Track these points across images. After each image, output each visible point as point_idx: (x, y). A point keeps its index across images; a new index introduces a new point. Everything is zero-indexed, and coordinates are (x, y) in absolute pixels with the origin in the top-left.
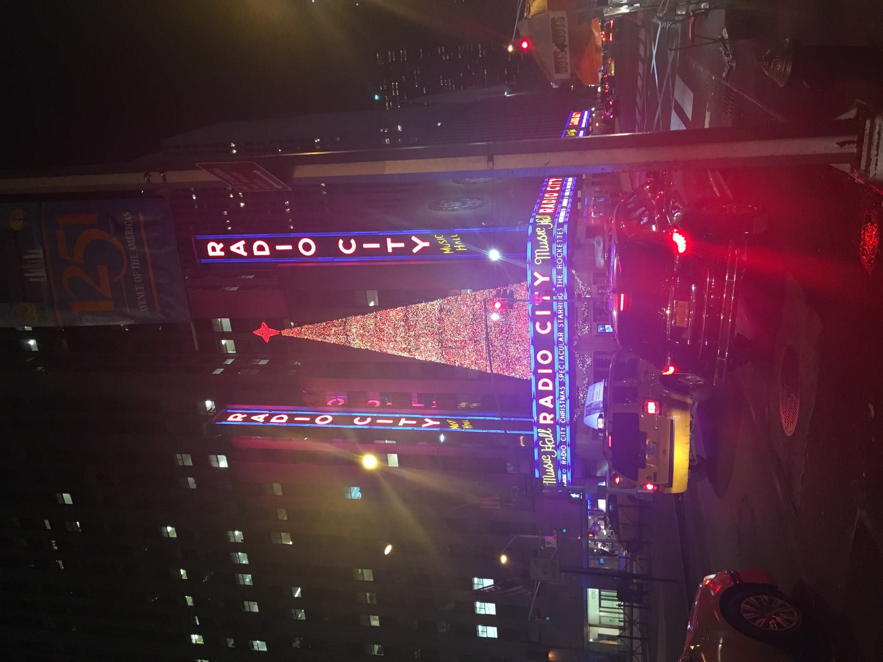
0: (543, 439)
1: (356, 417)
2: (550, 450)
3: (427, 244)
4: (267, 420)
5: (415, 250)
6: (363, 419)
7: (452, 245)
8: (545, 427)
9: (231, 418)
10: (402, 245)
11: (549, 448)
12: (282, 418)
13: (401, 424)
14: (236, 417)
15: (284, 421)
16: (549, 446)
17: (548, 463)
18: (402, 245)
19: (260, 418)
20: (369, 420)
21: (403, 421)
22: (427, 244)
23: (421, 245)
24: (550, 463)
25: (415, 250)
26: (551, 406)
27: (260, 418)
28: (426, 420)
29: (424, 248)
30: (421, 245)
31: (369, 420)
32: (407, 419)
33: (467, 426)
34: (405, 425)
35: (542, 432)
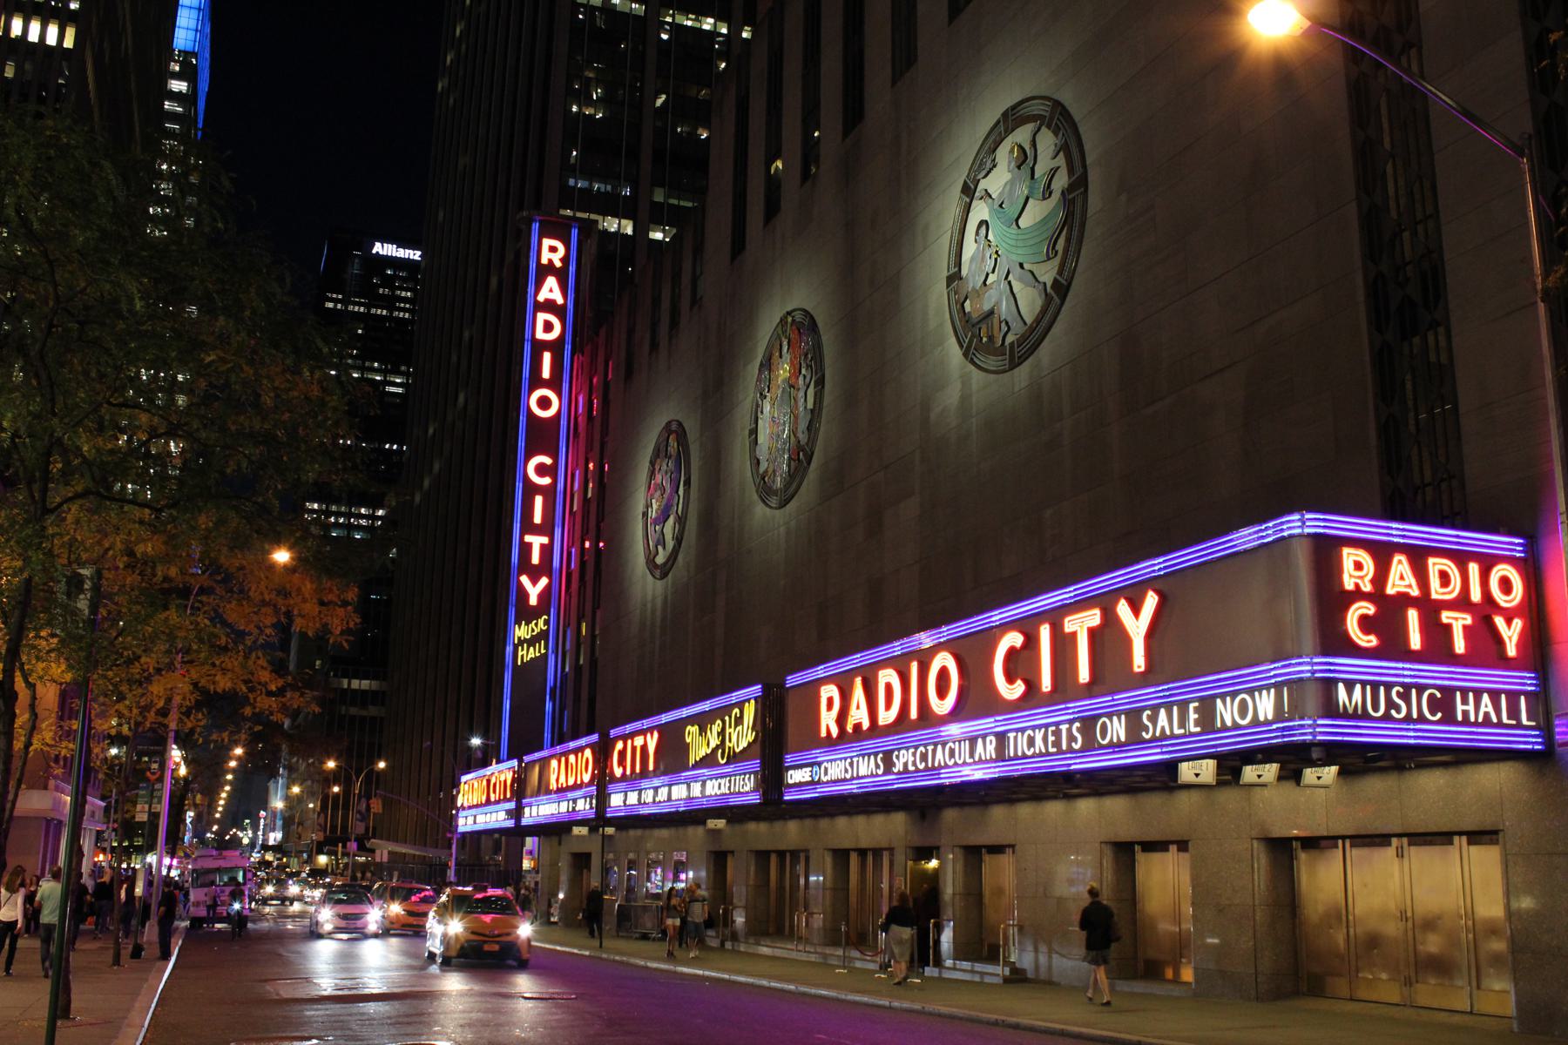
1: (554, 455)
4: (549, 306)
6: (541, 470)
9: (547, 242)
12: (548, 327)
13: (528, 538)
14: (553, 249)
15: (540, 335)
19: (551, 290)
20: (546, 481)
21: (537, 541)
27: (551, 290)
28: (544, 581)
31: (546, 481)
32: (546, 551)
34: (526, 549)
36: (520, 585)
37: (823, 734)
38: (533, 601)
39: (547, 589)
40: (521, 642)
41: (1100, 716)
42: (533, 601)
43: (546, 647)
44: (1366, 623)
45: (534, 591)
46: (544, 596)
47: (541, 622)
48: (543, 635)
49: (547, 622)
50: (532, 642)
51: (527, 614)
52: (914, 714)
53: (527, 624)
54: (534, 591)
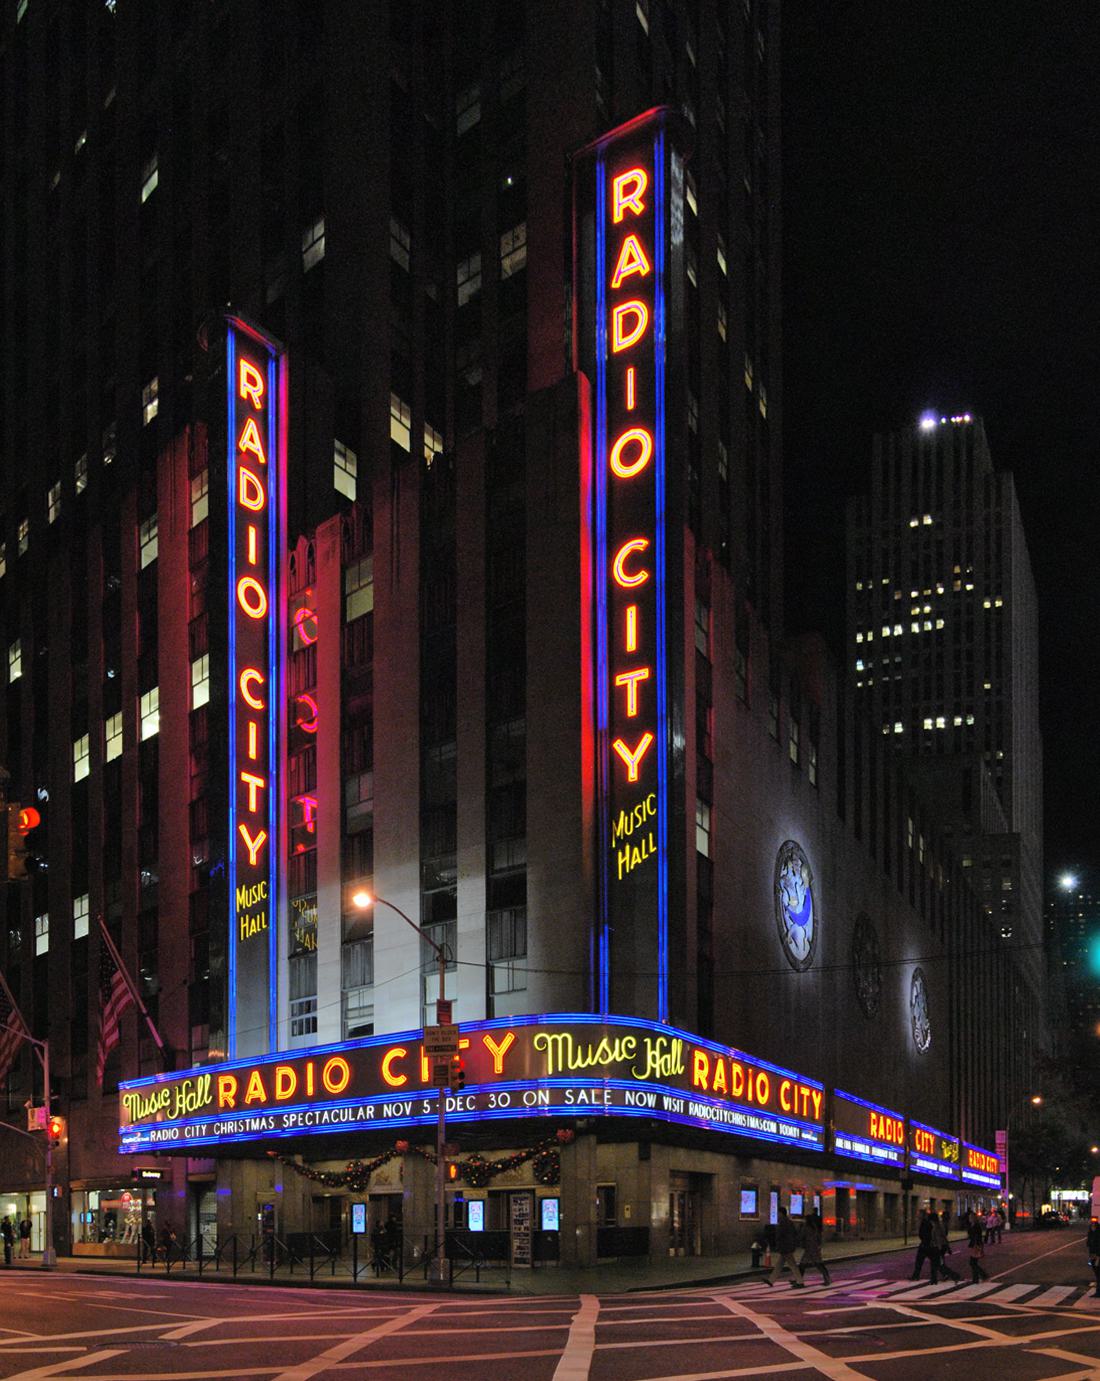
0: (193, 1088)
2: (178, 1105)
3: (633, 775)
5: (620, 747)
7: (634, 840)
8: (213, 1090)
10: (632, 710)
11: (181, 1102)
16: (183, 1104)
17: (159, 1102)
18: (632, 710)
22: (633, 775)
23: (631, 759)
24: (158, 1106)
25: (620, 747)
26: (248, 1101)
29: (625, 767)
30: (631, 759)
33: (251, 927)
35: (204, 1083)
36: (238, 833)
37: (222, 1103)
38: (253, 860)
39: (266, 844)
40: (244, 912)
41: (400, 1117)
42: (253, 860)
43: (267, 922)
44: (397, 1067)
45: (253, 847)
46: (264, 852)
47: (260, 887)
48: (264, 906)
49: (266, 890)
50: (252, 912)
51: (248, 878)
52: (310, 1090)
53: (248, 889)
54: (253, 847)
